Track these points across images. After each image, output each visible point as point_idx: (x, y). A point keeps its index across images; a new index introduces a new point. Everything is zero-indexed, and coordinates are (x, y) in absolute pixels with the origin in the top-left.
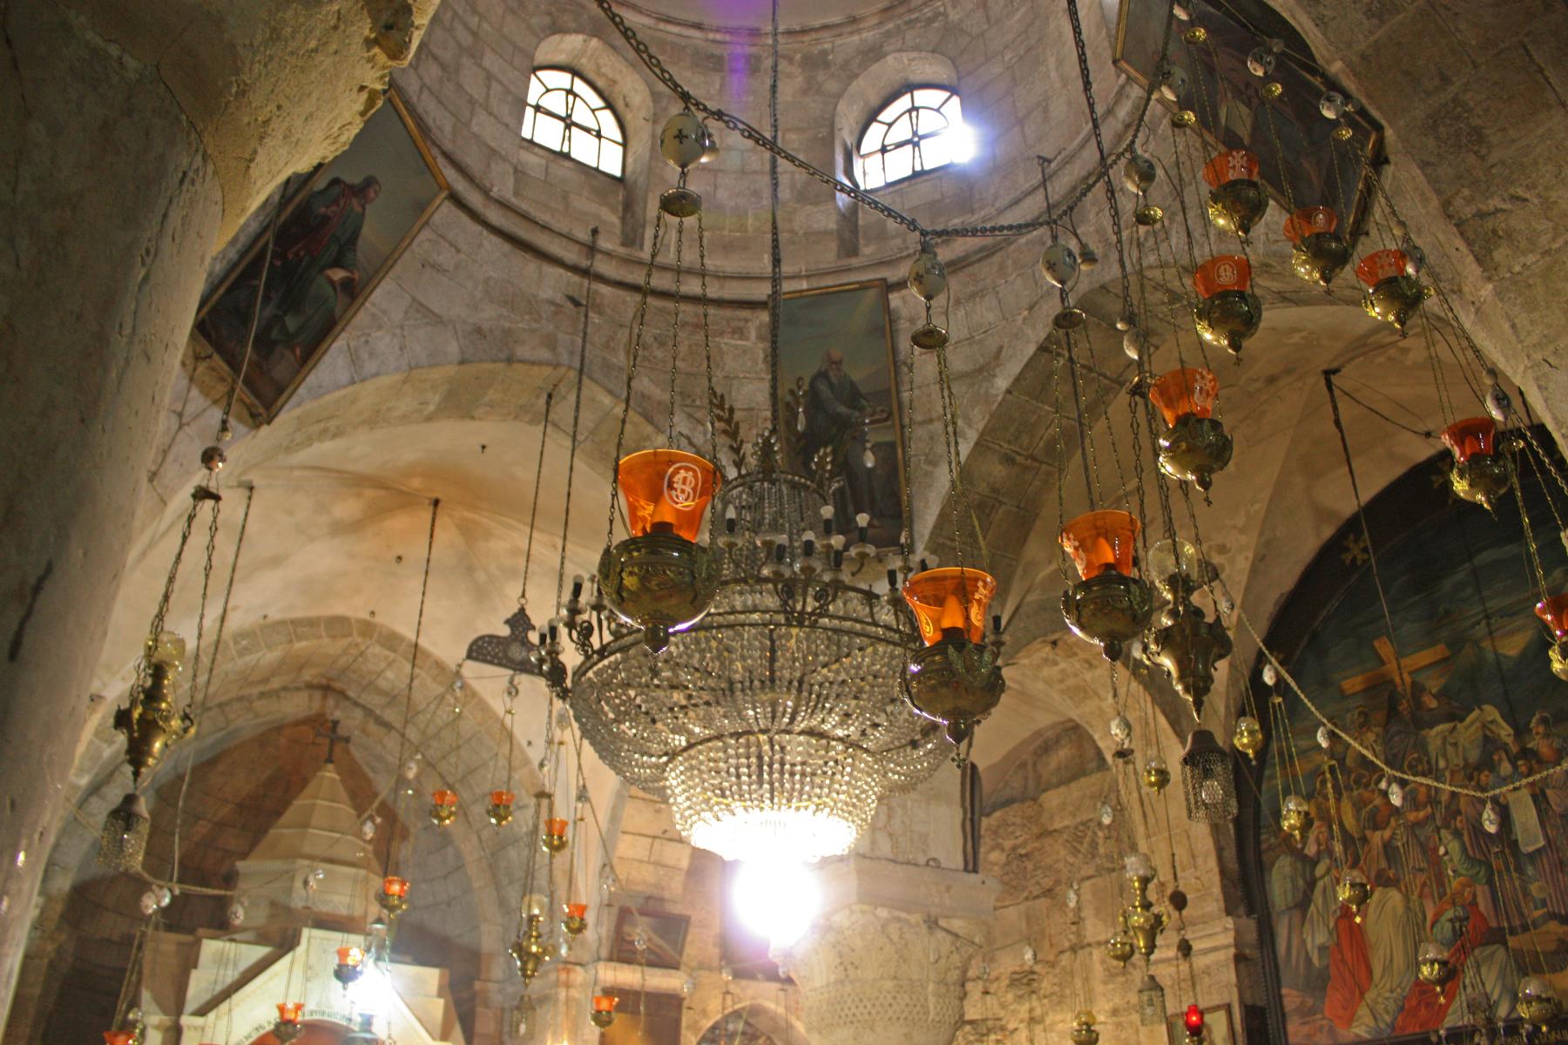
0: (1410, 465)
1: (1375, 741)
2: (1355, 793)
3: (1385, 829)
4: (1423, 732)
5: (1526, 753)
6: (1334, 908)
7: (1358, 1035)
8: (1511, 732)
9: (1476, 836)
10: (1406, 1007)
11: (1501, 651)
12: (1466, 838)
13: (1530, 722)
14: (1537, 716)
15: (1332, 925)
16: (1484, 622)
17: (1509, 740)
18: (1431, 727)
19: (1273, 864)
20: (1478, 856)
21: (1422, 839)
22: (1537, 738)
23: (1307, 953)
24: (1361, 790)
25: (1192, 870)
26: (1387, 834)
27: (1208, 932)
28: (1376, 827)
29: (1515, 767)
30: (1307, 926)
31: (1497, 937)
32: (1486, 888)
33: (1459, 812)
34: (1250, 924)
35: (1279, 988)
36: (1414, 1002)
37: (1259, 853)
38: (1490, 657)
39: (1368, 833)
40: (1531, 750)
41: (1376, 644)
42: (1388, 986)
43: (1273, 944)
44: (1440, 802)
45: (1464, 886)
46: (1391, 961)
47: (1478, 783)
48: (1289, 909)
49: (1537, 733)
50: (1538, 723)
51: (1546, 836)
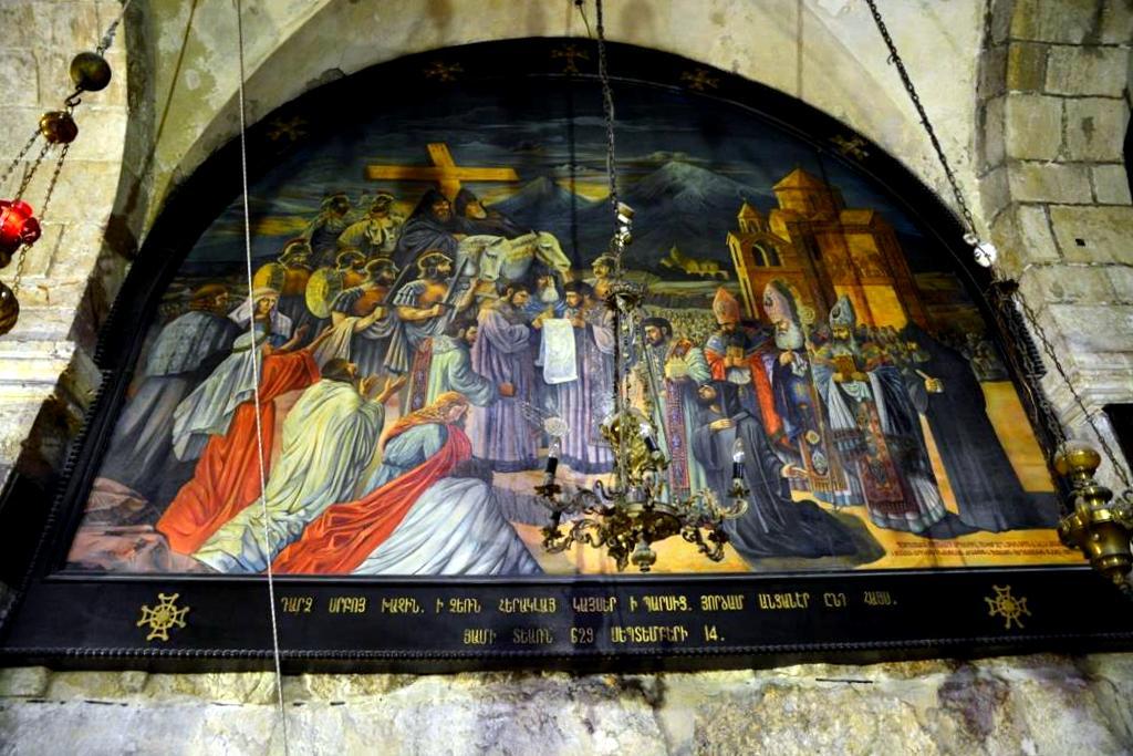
0: (536, 33)
1: (389, 229)
2: (338, 270)
3: (363, 317)
4: (457, 236)
5: (579, 286)
6: (243, 389)
7: (202, 565)
8: (569, 263)
9: (488, 351)
10: (305, 537)
11: (578, 193)
12: (474, 350)
13: (593, 261)
14: (604, 258)
15: (230, 407)
16: (567, 166)
17: (564, 271)
18: (469, 234)
19: (172, 317)
20: (483, 374)
21: (412, 339)
22: (598, 276)
23: (170, 437)
24: (347, 270)
25: (43, 276)
26: (364, 323)
27: (18, 354)
28: (350, 312)
29: (562, 296)
30: (188, 402)
31: (482, 470)
32: (483, 411)
33: (475, 323)
34: (91, 381)
35: (96, 473)
36: (321, 533)
37: (156, 299)
38: (565, 193)
39: (336, 316)
40: (588, 285)
41: (430, 147)
42: (285, 506)
43: (118, 414)
44: (453, 307)
45: (452, 402)
46: (306, 471)
47: (511, 300)
48: (168, 376)
49: (599, 272)
50: (603, 263)
51: (581, 372)
